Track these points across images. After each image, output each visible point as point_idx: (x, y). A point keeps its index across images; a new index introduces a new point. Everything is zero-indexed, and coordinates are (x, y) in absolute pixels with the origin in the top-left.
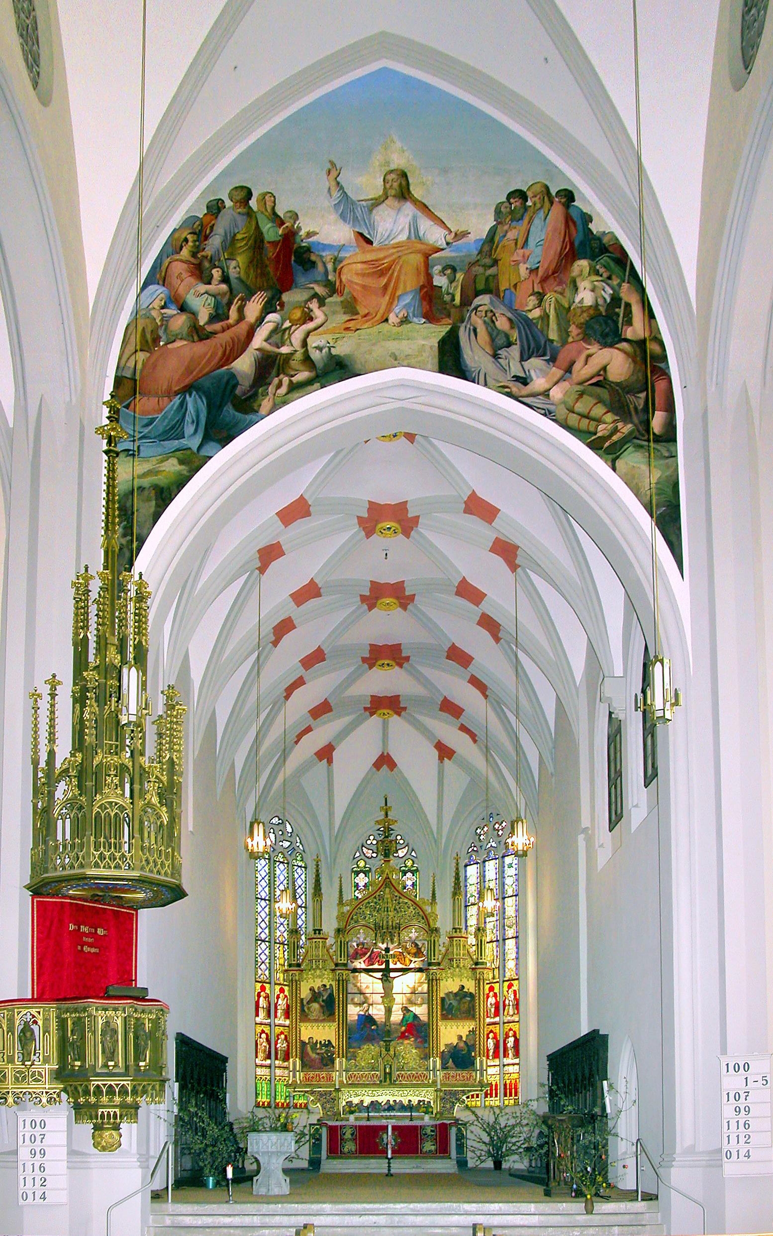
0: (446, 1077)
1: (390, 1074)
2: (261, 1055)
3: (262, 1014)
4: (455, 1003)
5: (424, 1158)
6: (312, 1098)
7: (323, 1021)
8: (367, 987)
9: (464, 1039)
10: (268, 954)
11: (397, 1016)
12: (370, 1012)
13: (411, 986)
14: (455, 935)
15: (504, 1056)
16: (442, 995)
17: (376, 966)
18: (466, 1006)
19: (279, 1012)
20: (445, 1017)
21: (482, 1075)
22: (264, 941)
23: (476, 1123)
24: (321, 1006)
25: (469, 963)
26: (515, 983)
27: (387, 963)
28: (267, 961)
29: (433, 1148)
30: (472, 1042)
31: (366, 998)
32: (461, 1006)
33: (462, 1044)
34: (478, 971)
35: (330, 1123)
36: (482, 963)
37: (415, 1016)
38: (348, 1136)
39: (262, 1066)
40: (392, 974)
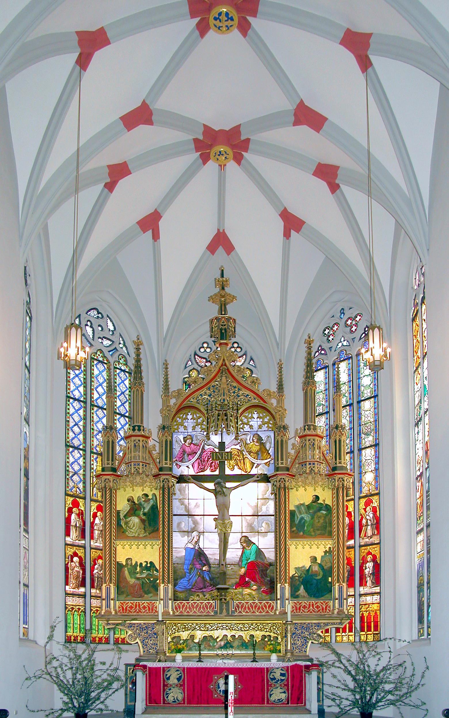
0: (296, 609)
2: (72, 580)
3: (74, 533)
4: (307, 517)
5: (272, 708)
6: (130, 632)
7: (145, 538)
9: (319, 561)
14: (307, 432)
15: (361, 585)
16: (292, 508)
18: (321, 521)
19: (96, 533)
20: (295, 535)
21: (341, 605)
22: (77, 448)
23: (337, 664)
25: (324, 469)
26: (375, 499)
28: (81, 472)
29: (283, 696)
30: (329, 565)
32: (315, 521)
33: (316, 568)
34: (337, 477)
35: (150, 664)
36: (342, 468)
38: (173, 680)
39: (73, 595)
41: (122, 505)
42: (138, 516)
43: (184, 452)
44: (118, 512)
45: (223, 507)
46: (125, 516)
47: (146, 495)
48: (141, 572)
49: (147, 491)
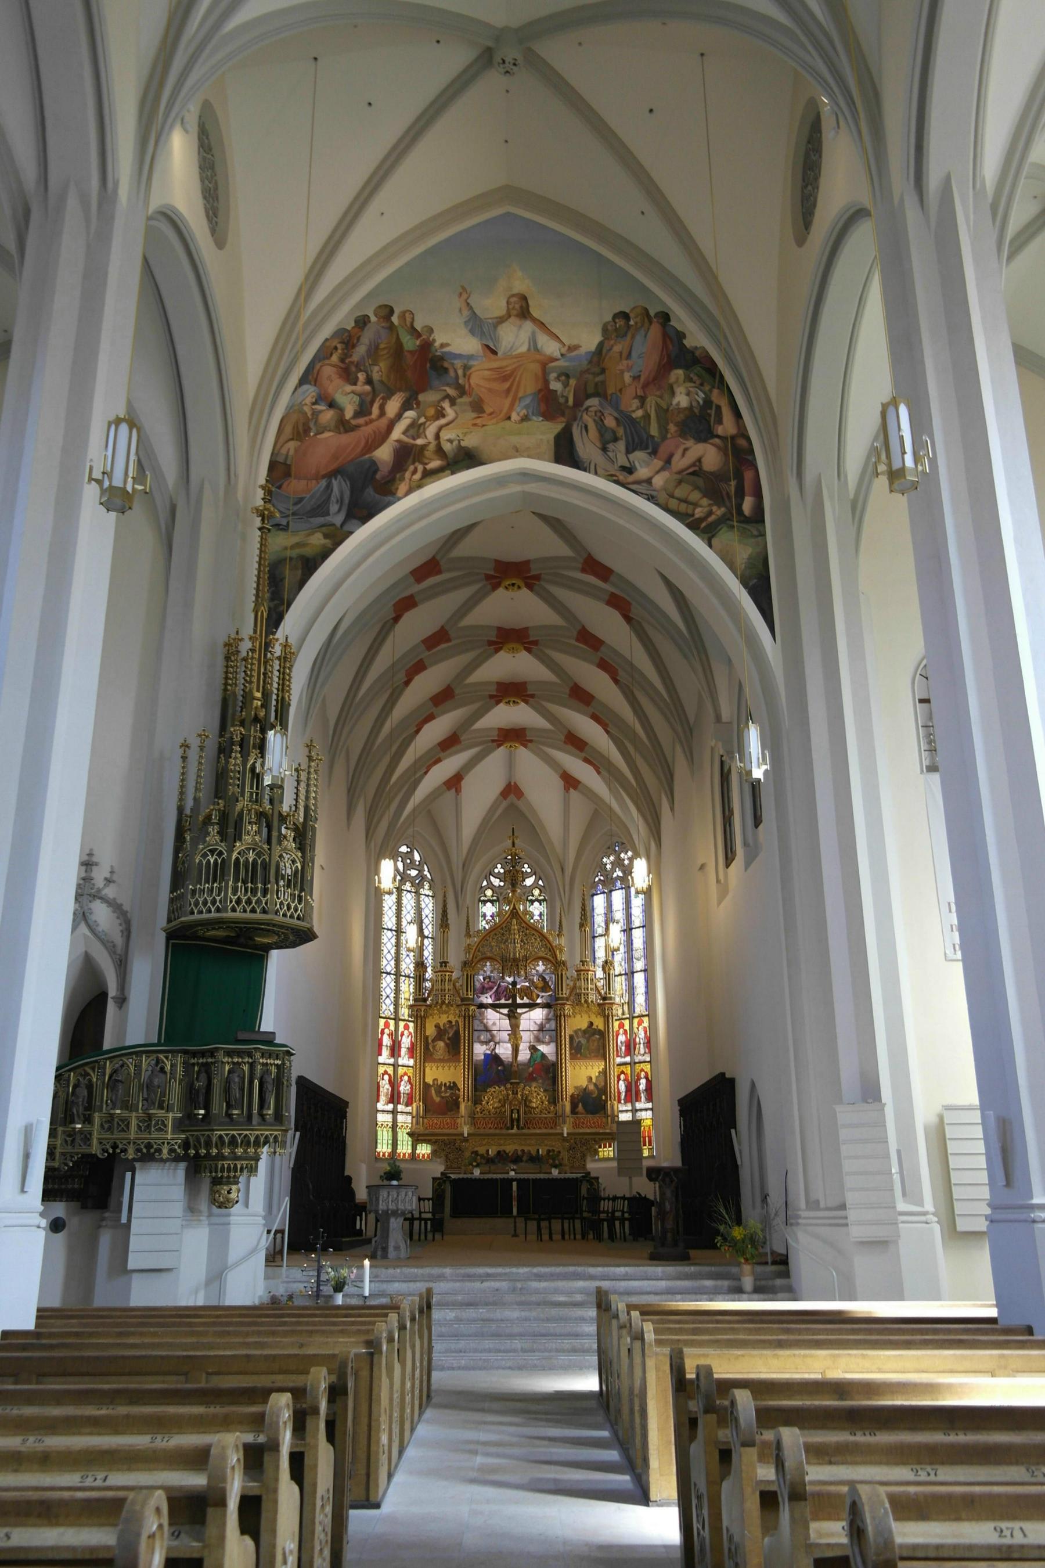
1: (518, 1120)
4: (583, 1041)
7: (448, 1061)
8: (494, 1024)
9: (594, 1080)
10: (393, 988)
11: (524, 1055)
12: (497, 1051)
13: (539, 1022)
17: (503, 1001)
18: (596, 1044)
20: (573, 1057)
24: (447, 1045)
27: (515, 999)
31: (493, 1036)
33: (591, 1087)
36: (611, 998)
37: (543, 1055)
40: (519, 1011)
41: (430, 1031)
42: (443, 1040)
43: (483, 987)
44: (427, 1038)
45: (515, 1028)
46: (433, 1041)
47: (450, 1022)
48: (446, 1092)
49: (452, 1018)
